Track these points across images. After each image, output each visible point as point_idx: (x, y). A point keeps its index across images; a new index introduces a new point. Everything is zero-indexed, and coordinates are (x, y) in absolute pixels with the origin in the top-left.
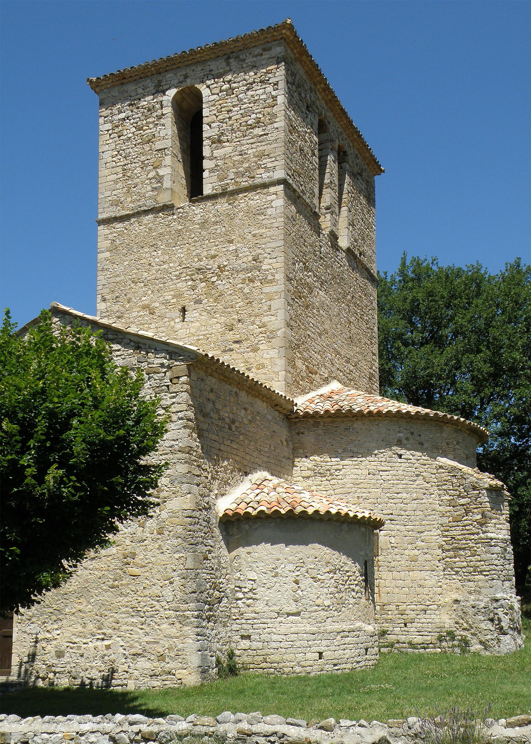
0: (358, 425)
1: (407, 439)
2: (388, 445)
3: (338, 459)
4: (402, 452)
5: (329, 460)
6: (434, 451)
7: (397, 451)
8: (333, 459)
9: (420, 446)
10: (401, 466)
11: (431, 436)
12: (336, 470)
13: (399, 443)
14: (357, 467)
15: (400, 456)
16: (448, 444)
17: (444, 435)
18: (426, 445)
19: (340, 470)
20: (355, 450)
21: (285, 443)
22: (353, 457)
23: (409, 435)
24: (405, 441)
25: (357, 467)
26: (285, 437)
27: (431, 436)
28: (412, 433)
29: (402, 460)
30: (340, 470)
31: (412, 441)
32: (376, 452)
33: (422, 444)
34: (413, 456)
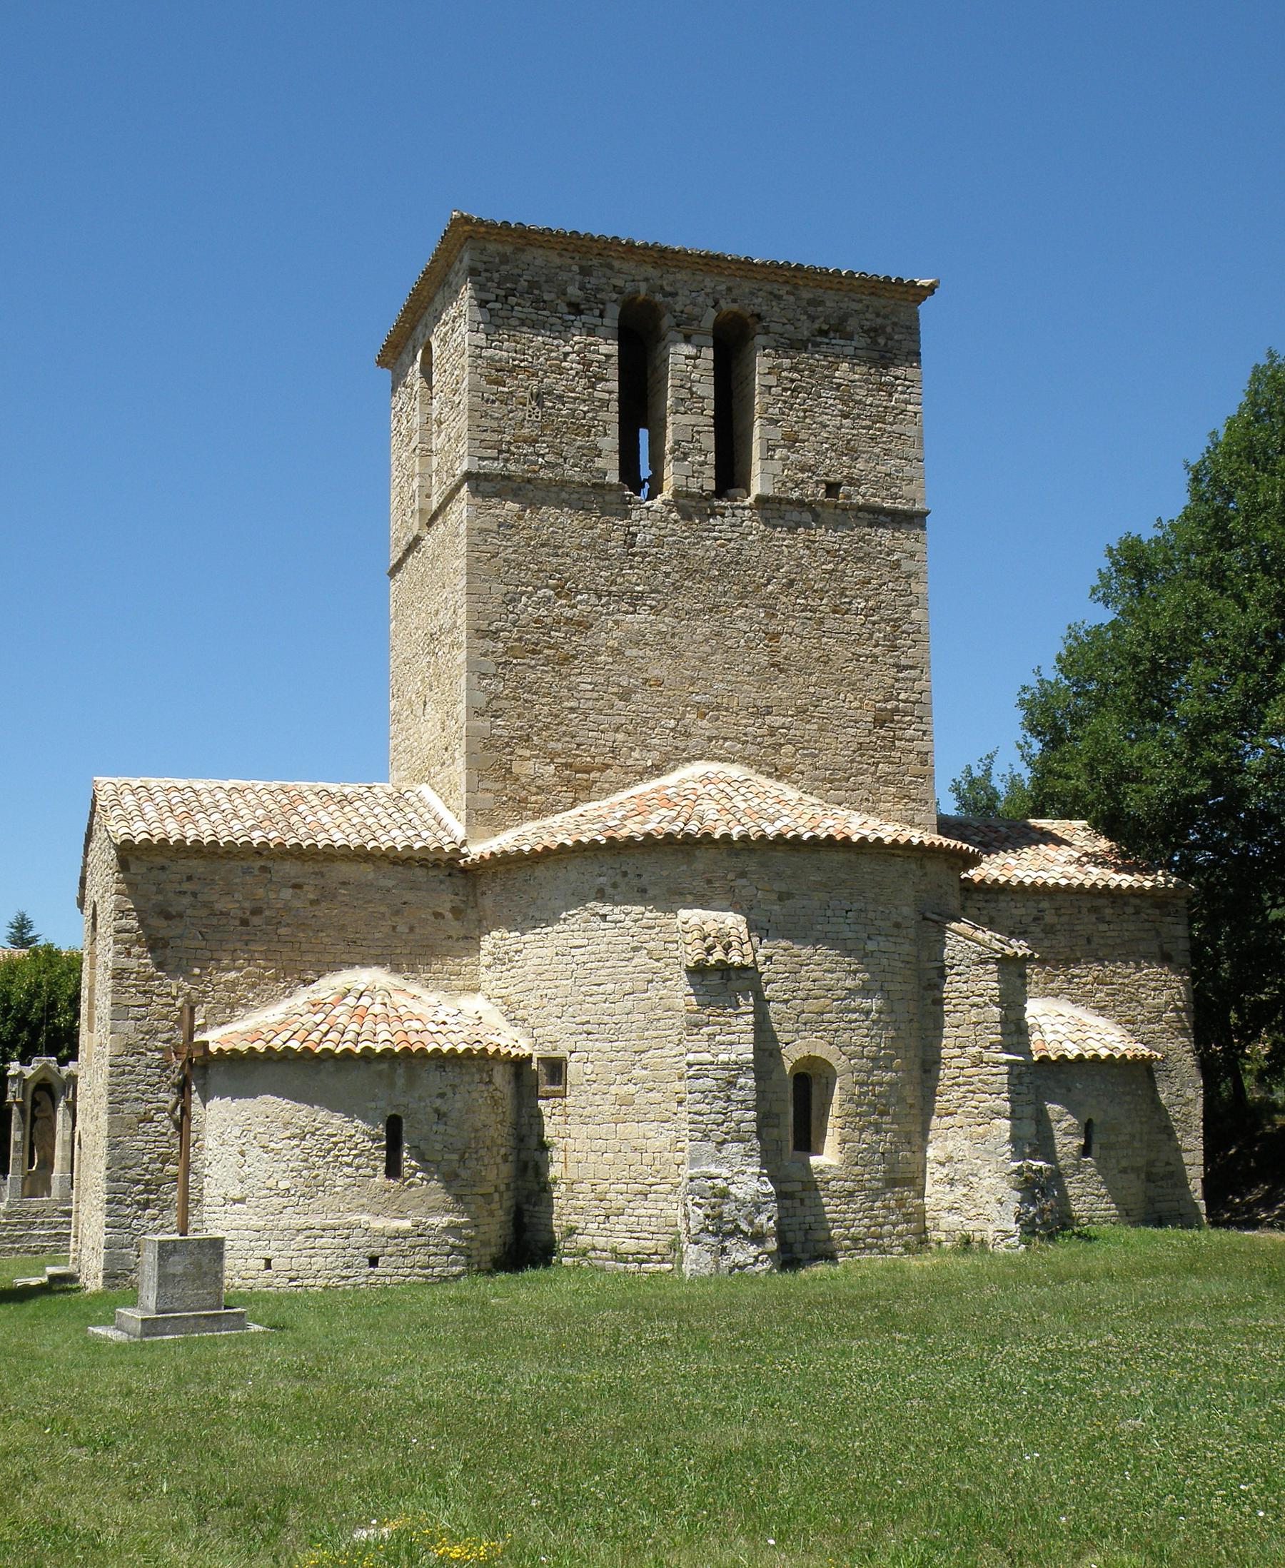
0: (540, 871)
1: (615, 886)
2: (580, 900)
3: (518, 934)
4: (606, 910)
5: (507, 935)
6: (672, 898)
7: (597, 910)
8: (513, 934)
9: (641, 895)
10: (604, 936)
11: (665, 873)
12: (516, 952)
13: (601, 896)
14: (541, 944)
15: (604, 917)
16: (709, 882)
17: (699, 866)
18: (651, 893)
19: (521, 951)
20: (537, 915)
21: (449, 915)
22: (535, 927)
23: (618, 878)
24: (609, 890)
25: (541, 944)
26: (448, 905)
27: (665, 873)
28: (625, 874)
29: (607, 925)
30: (521, 951)
31: (623, 888)
32: (563, 916)
33: (644, 891)
34: (627, 914)
